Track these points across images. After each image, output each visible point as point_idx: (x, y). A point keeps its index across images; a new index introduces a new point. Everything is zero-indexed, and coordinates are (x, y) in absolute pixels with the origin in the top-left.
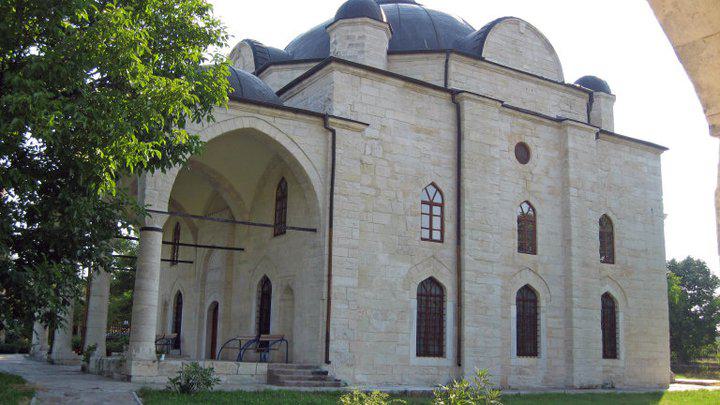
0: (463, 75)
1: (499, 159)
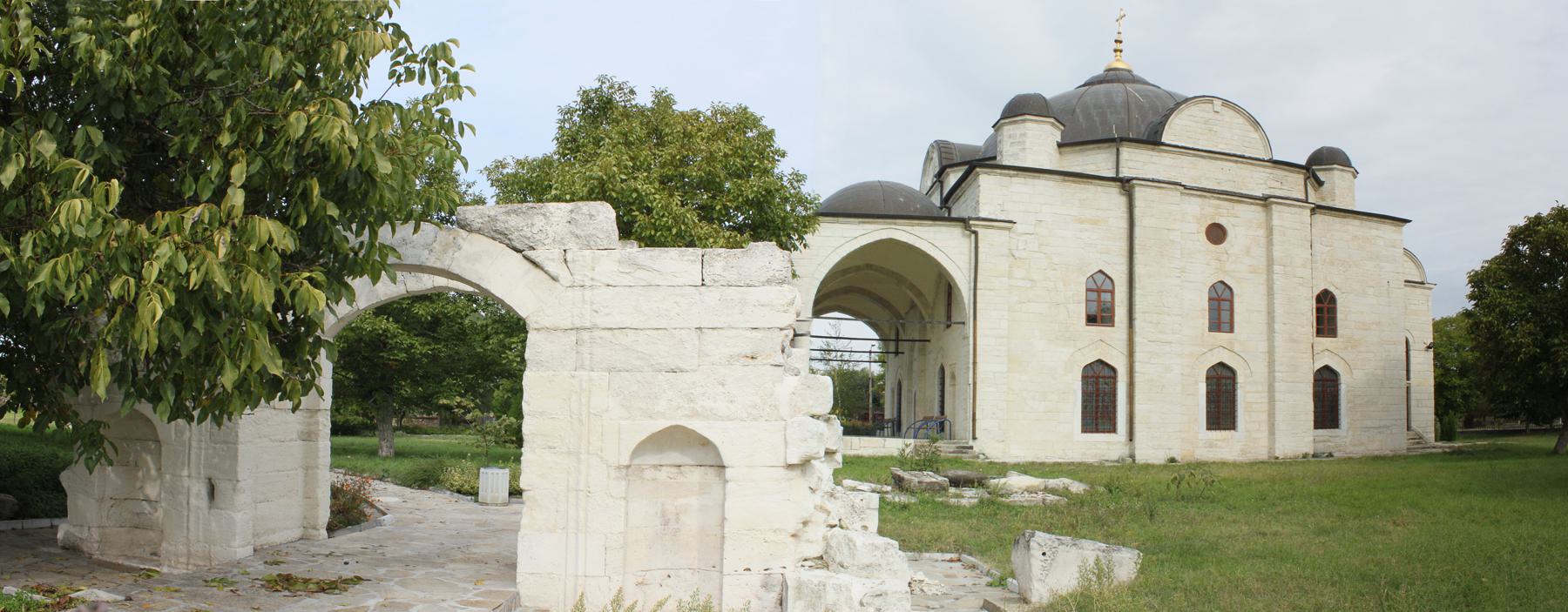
0: (1136, 161)
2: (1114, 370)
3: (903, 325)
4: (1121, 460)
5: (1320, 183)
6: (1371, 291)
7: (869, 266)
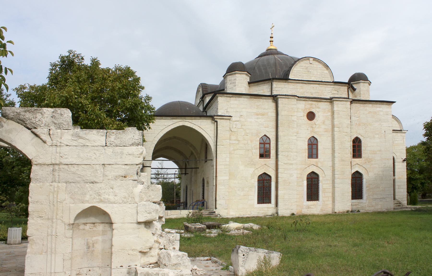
0: (279, 88)
1: (296, 121)
2: (270, 177)
3: (188, 162)
4: (272, 215)
5: (354, 90)
6: (377, 136)
7: (175, 137)
